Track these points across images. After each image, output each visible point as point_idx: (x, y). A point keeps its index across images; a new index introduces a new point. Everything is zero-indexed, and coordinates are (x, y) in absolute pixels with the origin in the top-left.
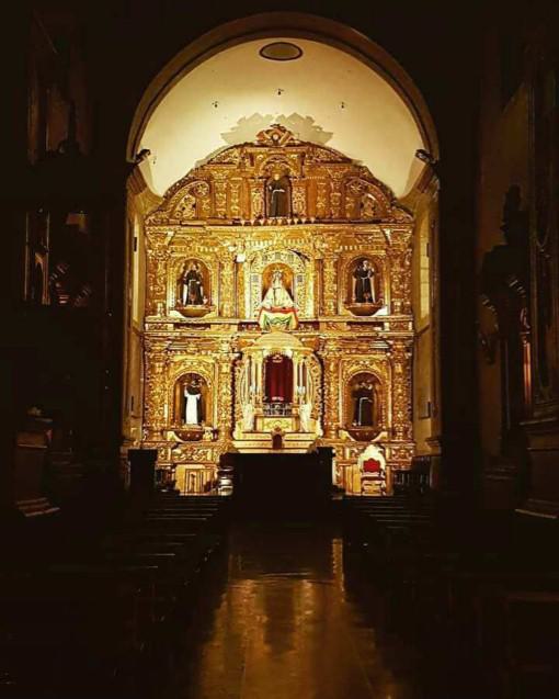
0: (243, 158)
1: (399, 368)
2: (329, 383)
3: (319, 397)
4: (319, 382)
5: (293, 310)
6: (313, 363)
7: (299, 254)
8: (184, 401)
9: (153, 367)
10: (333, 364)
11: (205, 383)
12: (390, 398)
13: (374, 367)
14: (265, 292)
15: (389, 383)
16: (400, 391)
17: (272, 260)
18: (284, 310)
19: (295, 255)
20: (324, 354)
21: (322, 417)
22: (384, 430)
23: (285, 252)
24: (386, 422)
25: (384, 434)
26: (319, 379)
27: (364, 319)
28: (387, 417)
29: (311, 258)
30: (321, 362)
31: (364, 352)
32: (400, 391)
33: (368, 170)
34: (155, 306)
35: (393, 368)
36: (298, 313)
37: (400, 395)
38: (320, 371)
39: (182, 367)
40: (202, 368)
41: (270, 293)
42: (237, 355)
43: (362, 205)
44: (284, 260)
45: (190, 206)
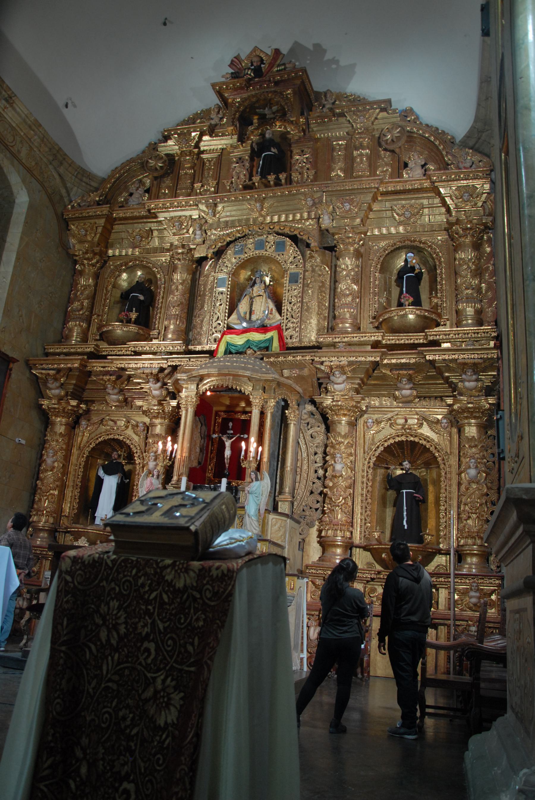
0: (221, 119)
1: (471, 431)
2: (334, 457)
3: (319, 483)
4: (319, 458)
5: (279, 328)
6: (312, 421)
7: (295, 239)
8: (100, 482)
9: (53, 424)
10: (344, 419)
11: (130, 457)
12: (455, 487)
13: (426, 431)
14: (232, 308)
15: (453, 461)
16: (472, 472)
17: (251, 252)
18: (264, 328)
19: (288, 241)
20: (328, 401)
21: (321, 521)
22: (439, 552)
23: (271, 238)
24: (447, 537)
25: (440, 560)
26: (320, 450)
27: (404, 339)
28: (448, 526)
29: (314, 244)
30: (325, 418)
31: (407, 402)
32: (472, 472)
33: (411, 110)
34: (71, 330)
35: (460, 431)
36: (285, 334)
37: (470, 482)
38: (320, 438)
39: (103, 428)
40: (130, 432)
41: (243, 307)
42: (174, 403)
43: (406, 165)
44: (270, 251)
45: (141, 191)
